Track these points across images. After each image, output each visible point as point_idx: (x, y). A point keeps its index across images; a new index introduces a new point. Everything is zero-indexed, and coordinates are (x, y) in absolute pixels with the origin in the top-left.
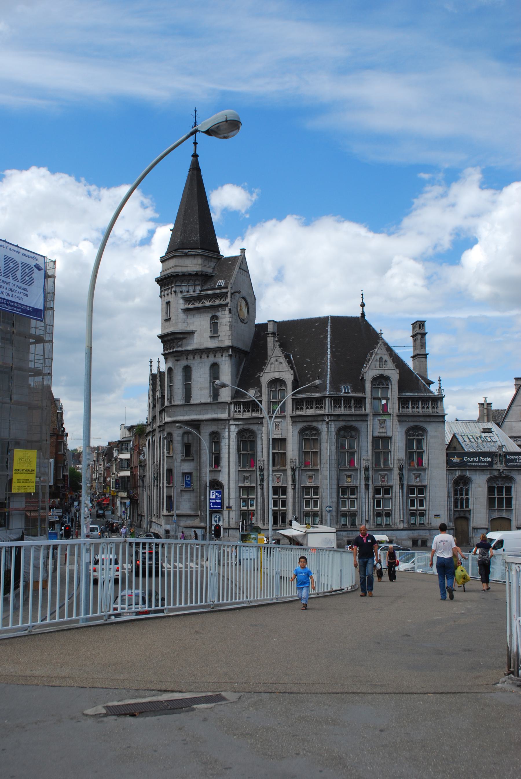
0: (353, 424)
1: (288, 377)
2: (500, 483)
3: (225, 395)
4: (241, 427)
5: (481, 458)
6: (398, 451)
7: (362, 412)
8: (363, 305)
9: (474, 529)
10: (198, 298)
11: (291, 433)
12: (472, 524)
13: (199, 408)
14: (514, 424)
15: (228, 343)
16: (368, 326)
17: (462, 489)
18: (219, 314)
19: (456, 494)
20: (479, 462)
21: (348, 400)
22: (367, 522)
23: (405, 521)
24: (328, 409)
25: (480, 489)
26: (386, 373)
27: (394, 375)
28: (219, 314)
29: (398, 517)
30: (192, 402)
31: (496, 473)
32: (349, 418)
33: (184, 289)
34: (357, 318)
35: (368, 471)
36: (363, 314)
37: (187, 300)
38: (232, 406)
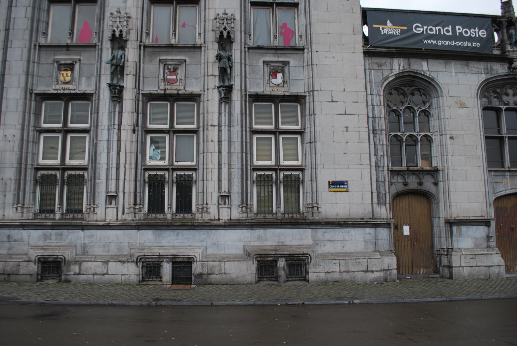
5: (459, 30)
9: (451, 223)
12: (443, 213)
20: (454, 37)
22: (111, 199)
23: (236, 198)
29: (212, 187)
35: (123, 48)
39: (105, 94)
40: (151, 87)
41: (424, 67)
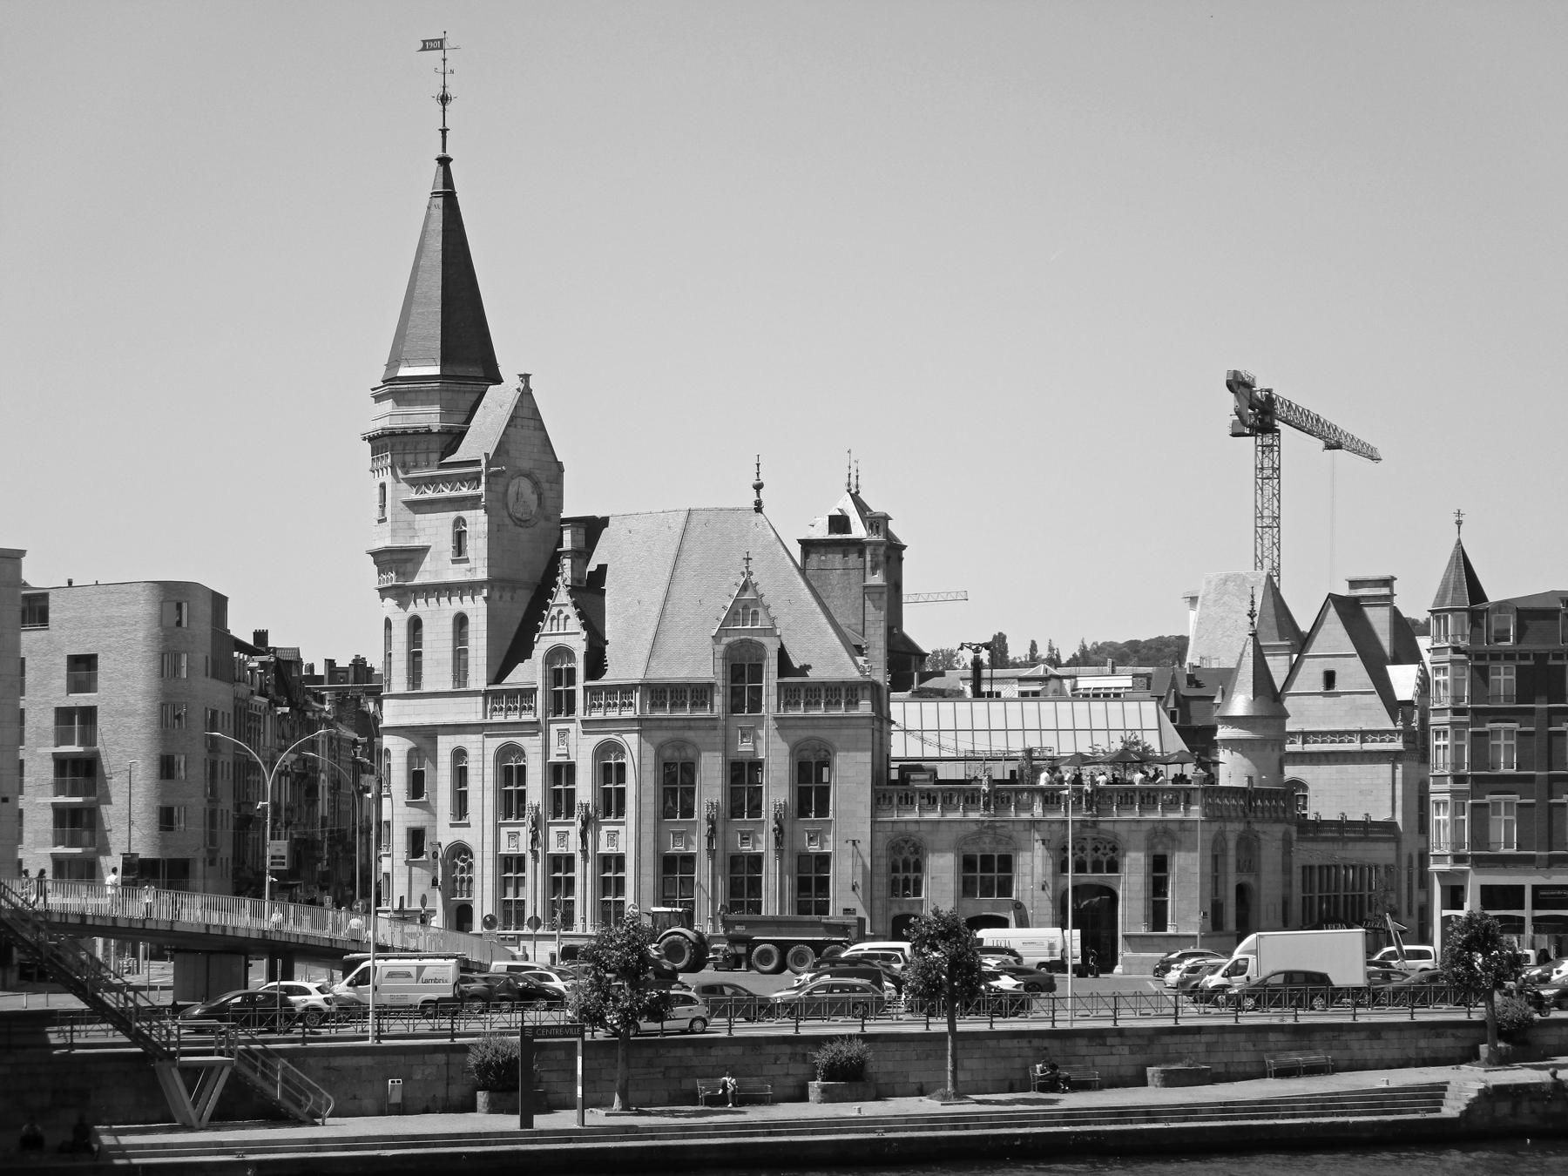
1: (579, 645)
2: (987, 846)
3: (478, 678)
6: (776, 790)
15: (482, 575)
19: (895, 869)
30: (426, 688)
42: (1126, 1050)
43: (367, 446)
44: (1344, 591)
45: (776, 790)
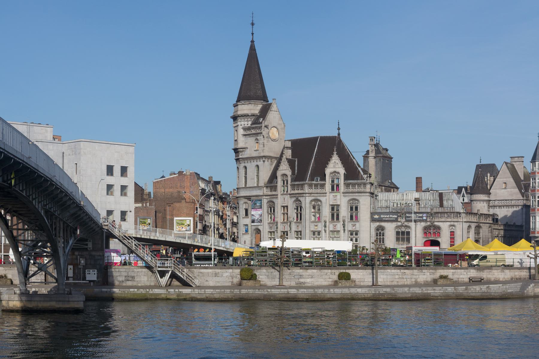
0: (319, 198)
1: (289, 173)
2: (403, 229)
4: (269, 200)
5: (391, 216)
6: (344, 212)
7: (324, 191)
8: (339, 129)
10: (249, 129)
11: (290, 202)
13: (251, 189)
14: (498, 191)
16: (340, 141)
17: (380, 233)
18: (258, 138)
19: (377, 236)
20: (390, 218)
21: (316, 185)
24: (307, 189)
25: (390, 233)
26: (337, 170)
27: (342, 171)
28: (258, 138)
31: (399, 224)
32: (316, 195)
33: (243, 123)
34: (336, 137)
36: (339, 134)
37: (245, 129)
38: (265, 188)
39: (324, 231)
40: (331, 229)
41: (383, 224)
42: (429, 274)
43: (232, 120)
44: (509, 160)
45: (344, 212)
